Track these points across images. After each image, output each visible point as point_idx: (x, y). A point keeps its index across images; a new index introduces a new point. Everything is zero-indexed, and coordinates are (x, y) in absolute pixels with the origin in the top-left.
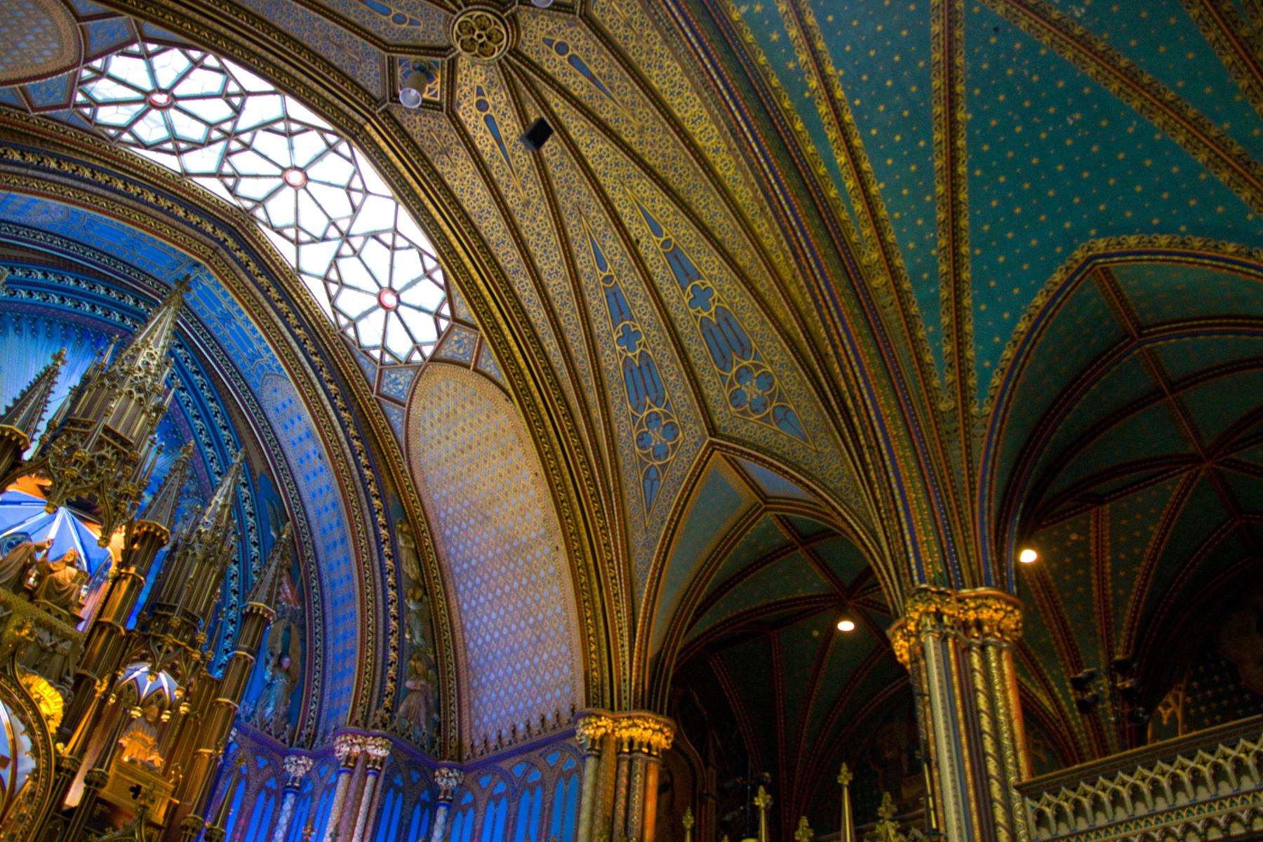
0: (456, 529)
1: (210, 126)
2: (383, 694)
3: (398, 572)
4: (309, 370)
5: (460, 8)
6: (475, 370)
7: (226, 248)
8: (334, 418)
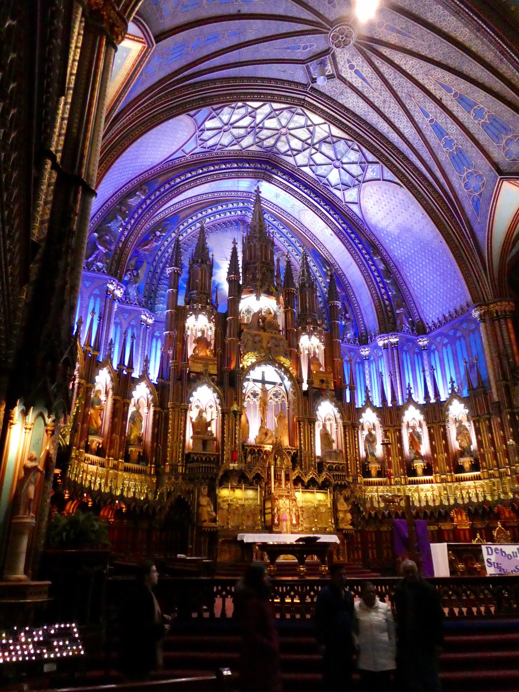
0: (395, 245)
1: (246, 127)
2: (389, 318)
3: (378, 270)
5: (329, 30)
6: (384, 180)
7: (268, 170)
8: (332, 219)
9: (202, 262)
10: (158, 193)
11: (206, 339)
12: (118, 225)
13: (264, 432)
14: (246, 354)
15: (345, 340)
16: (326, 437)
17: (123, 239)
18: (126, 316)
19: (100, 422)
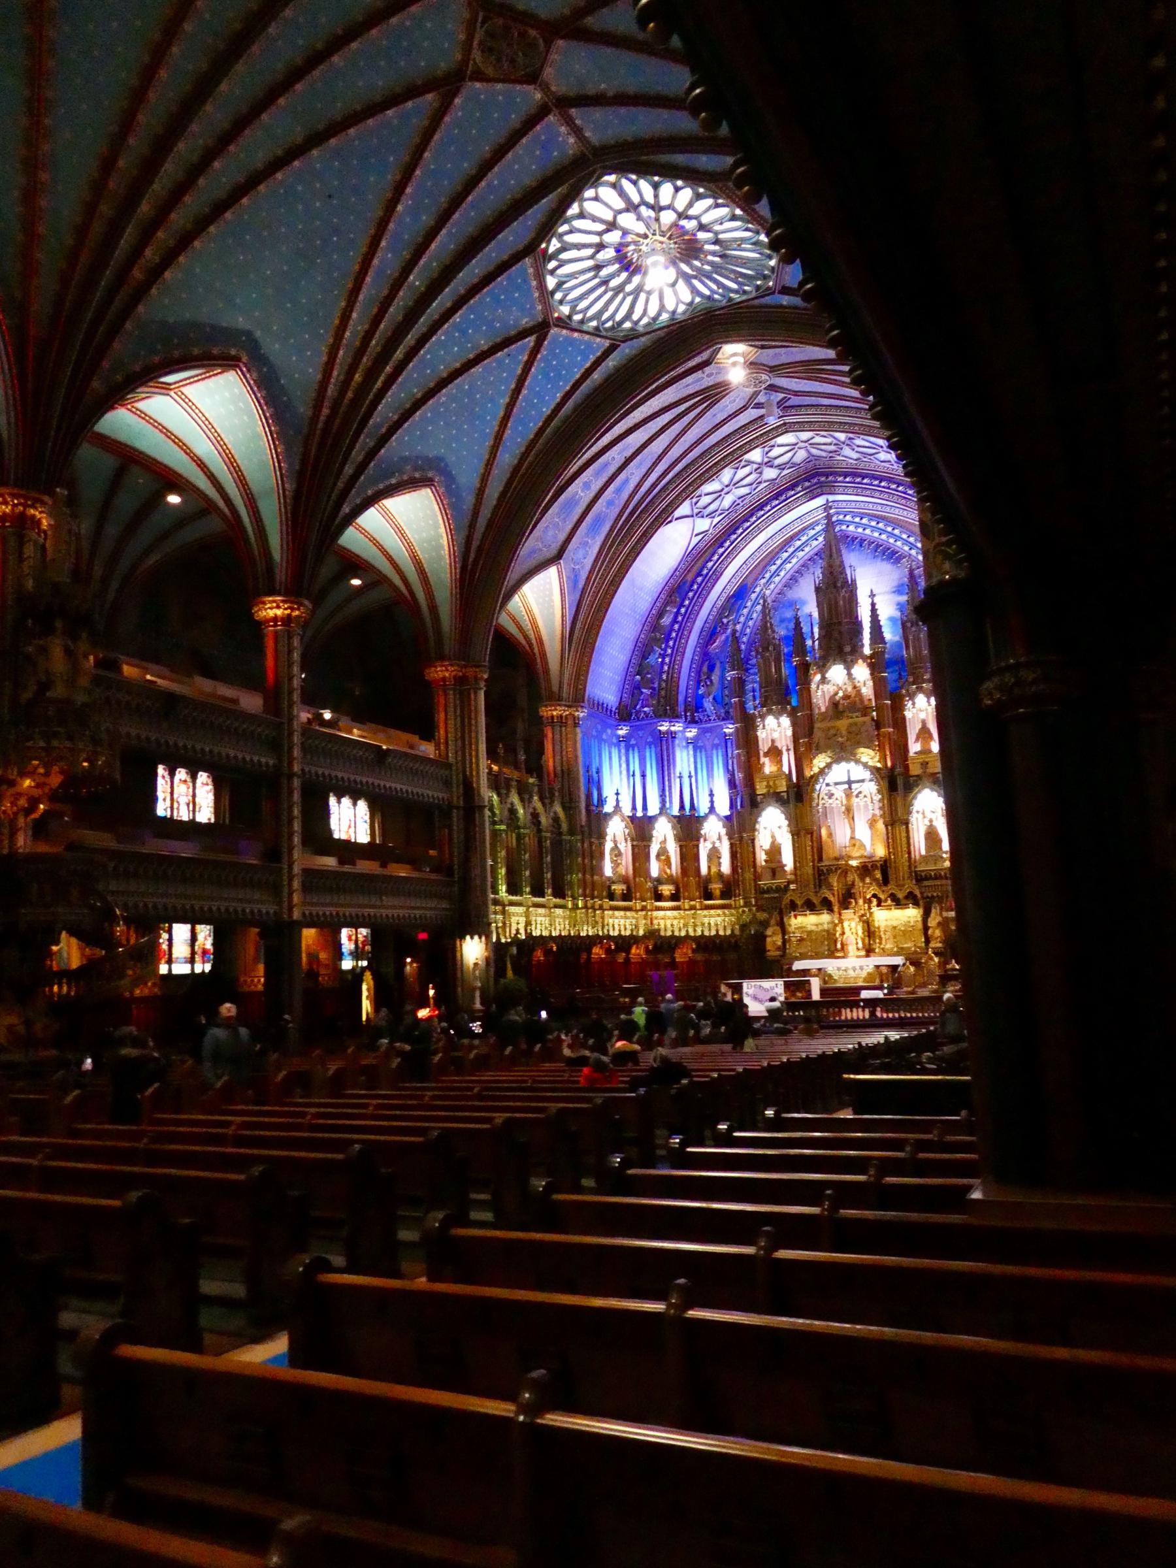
10: (691, 594)
11: (776, 748)
14: (814, 758)
17: (666, 668)
18: (708, 735)
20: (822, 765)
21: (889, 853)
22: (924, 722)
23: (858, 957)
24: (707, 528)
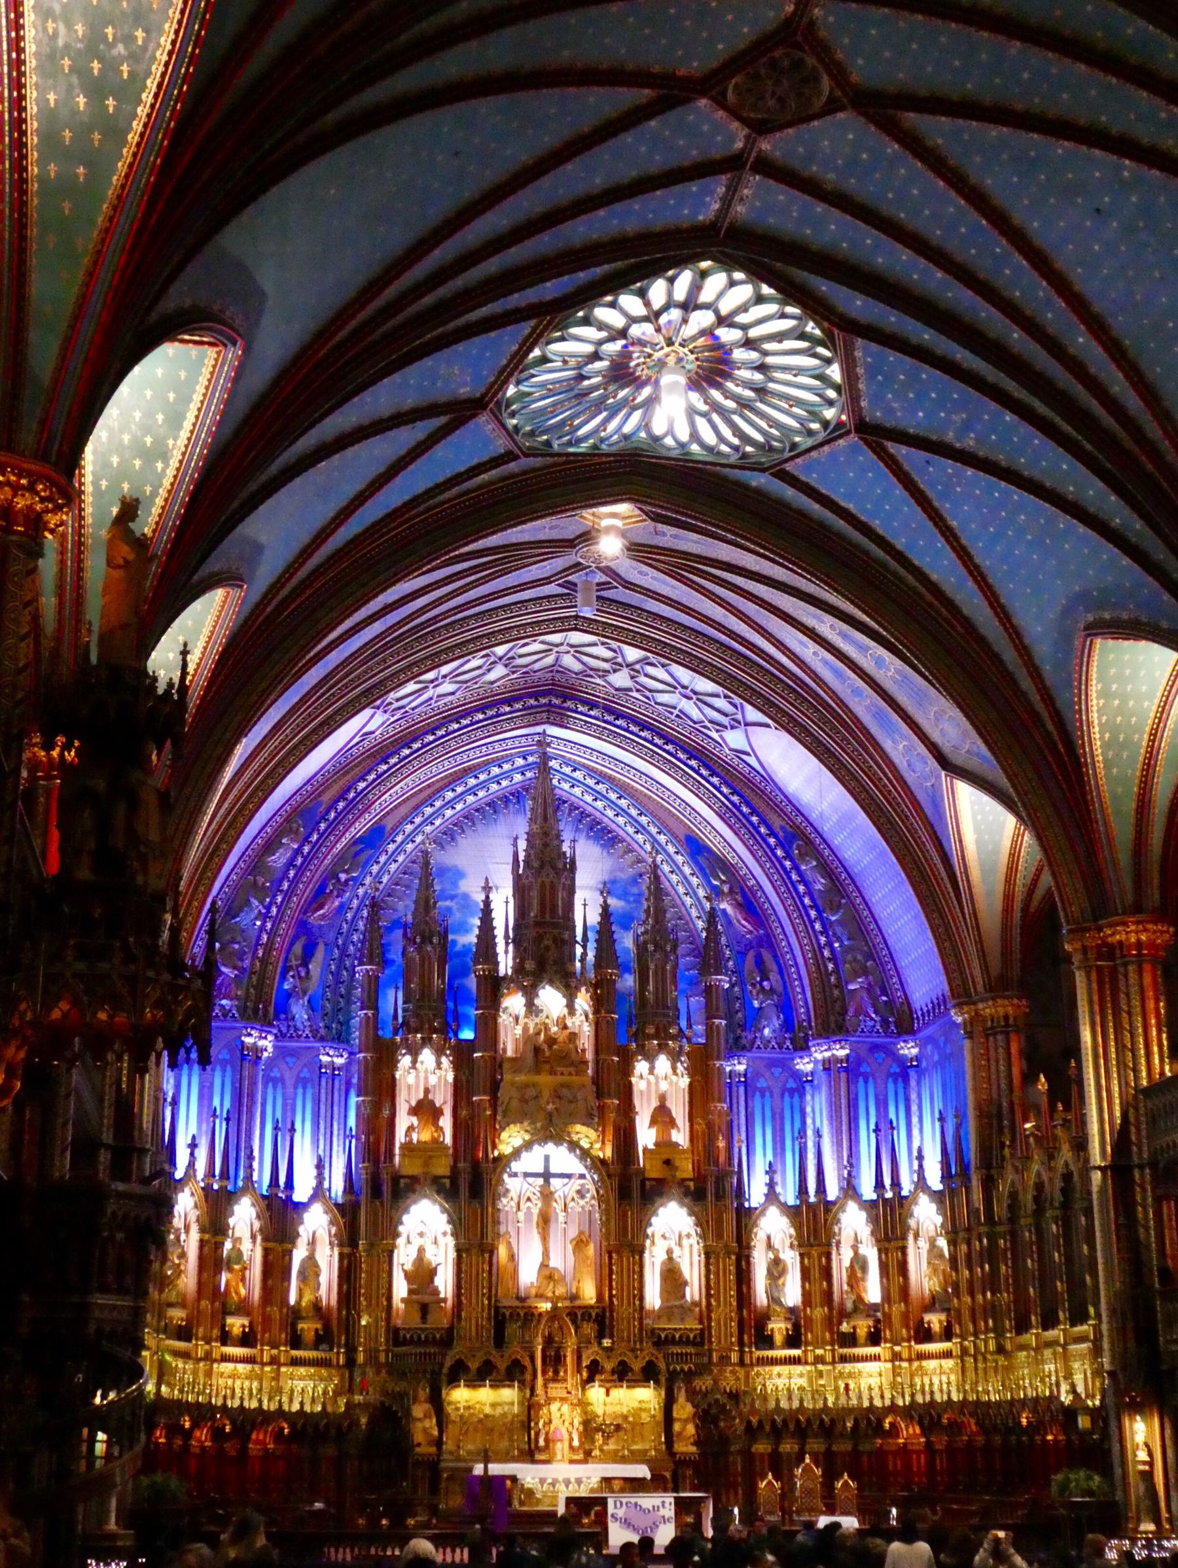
3: (810, 893)
4: (669, 757)
9: (423, 942)
11: (432, 1103)
12: (253, 916)
13: (547, 1274)
14: (503, 1129)
15: (758, 1042)
16: (672, 1277)
19: (243, 1292)
20: (517, 1141)
21: (611, 1296)
22: (663, 1098)
23: (572, 1462)
24: (372, 729)
